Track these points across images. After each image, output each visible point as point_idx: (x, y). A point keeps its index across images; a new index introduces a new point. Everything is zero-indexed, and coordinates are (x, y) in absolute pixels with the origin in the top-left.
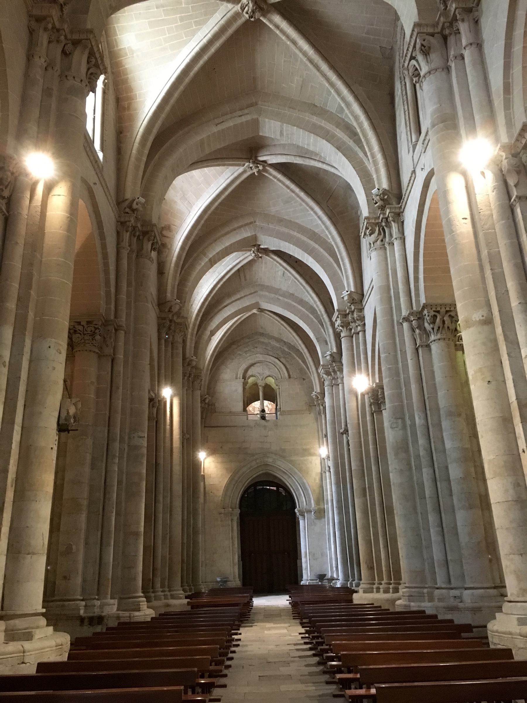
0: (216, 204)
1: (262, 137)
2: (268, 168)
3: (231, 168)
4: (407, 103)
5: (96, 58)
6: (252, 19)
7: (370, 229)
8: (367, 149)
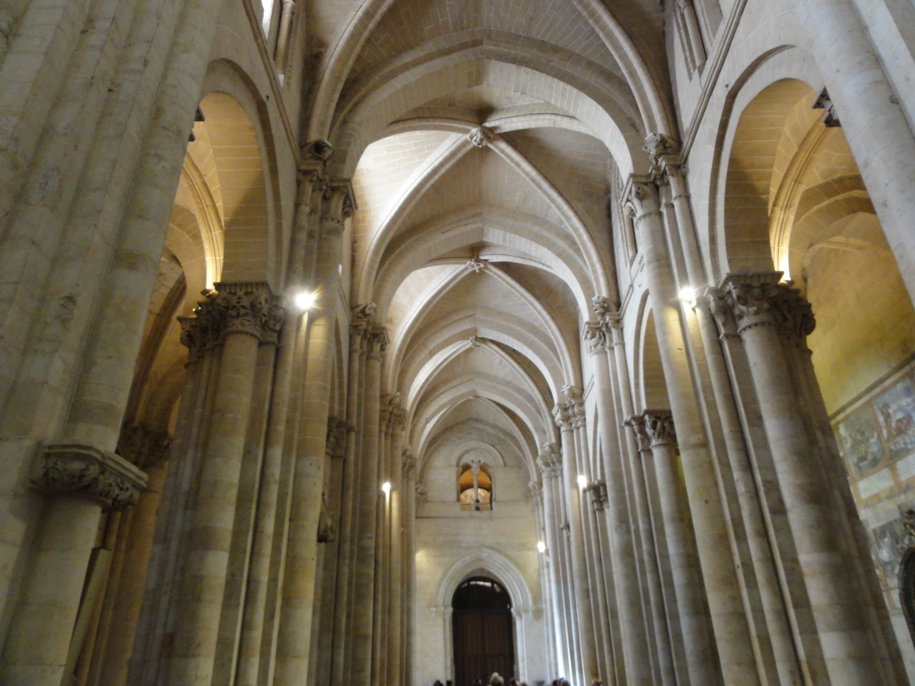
0: (438, 299)
1: (484, 242)
2: (489, 266)
6: (480, 146)
7: (591, 333)
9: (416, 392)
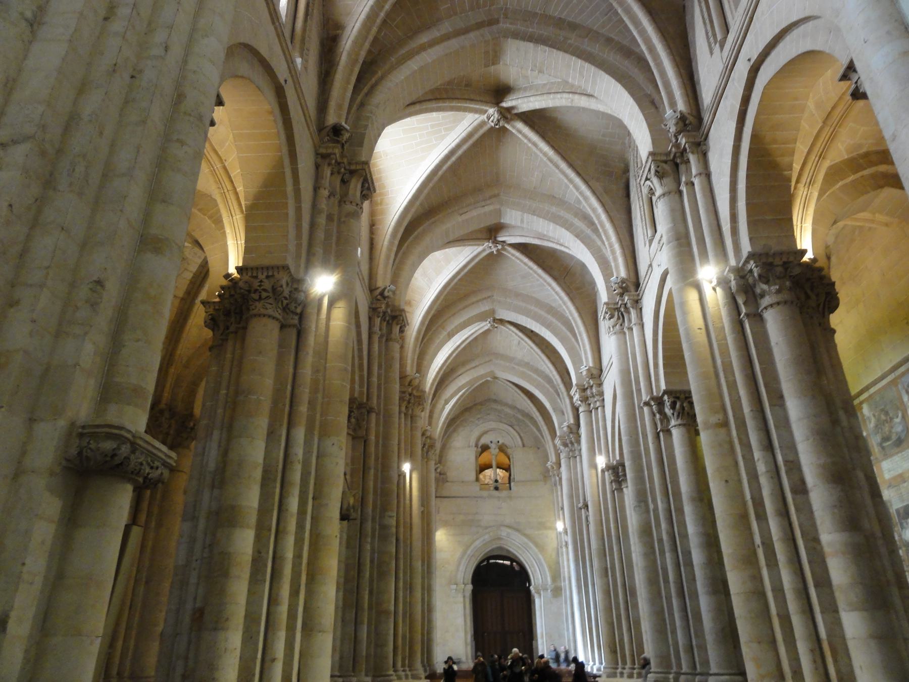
0: (456, 280)
1: (503, 223)
2: (507, 247)
3: (469, 247)
4: (642, 199)
5: (369, 183)
6: (497, 127)
8: (604, 239)
9: (435, 373)
